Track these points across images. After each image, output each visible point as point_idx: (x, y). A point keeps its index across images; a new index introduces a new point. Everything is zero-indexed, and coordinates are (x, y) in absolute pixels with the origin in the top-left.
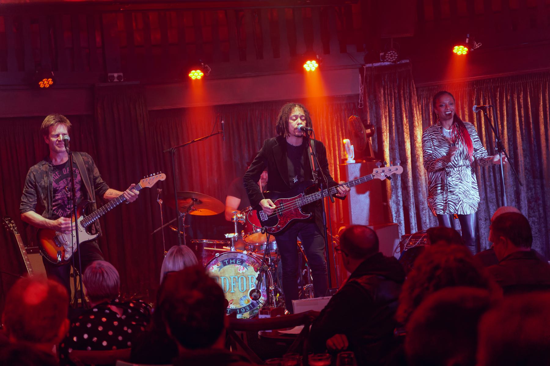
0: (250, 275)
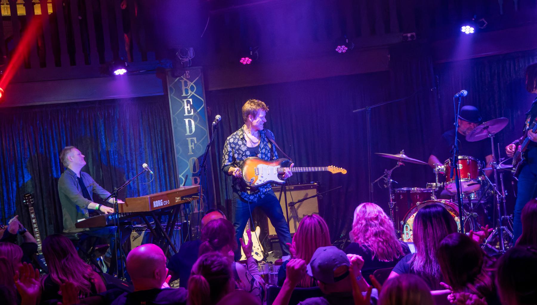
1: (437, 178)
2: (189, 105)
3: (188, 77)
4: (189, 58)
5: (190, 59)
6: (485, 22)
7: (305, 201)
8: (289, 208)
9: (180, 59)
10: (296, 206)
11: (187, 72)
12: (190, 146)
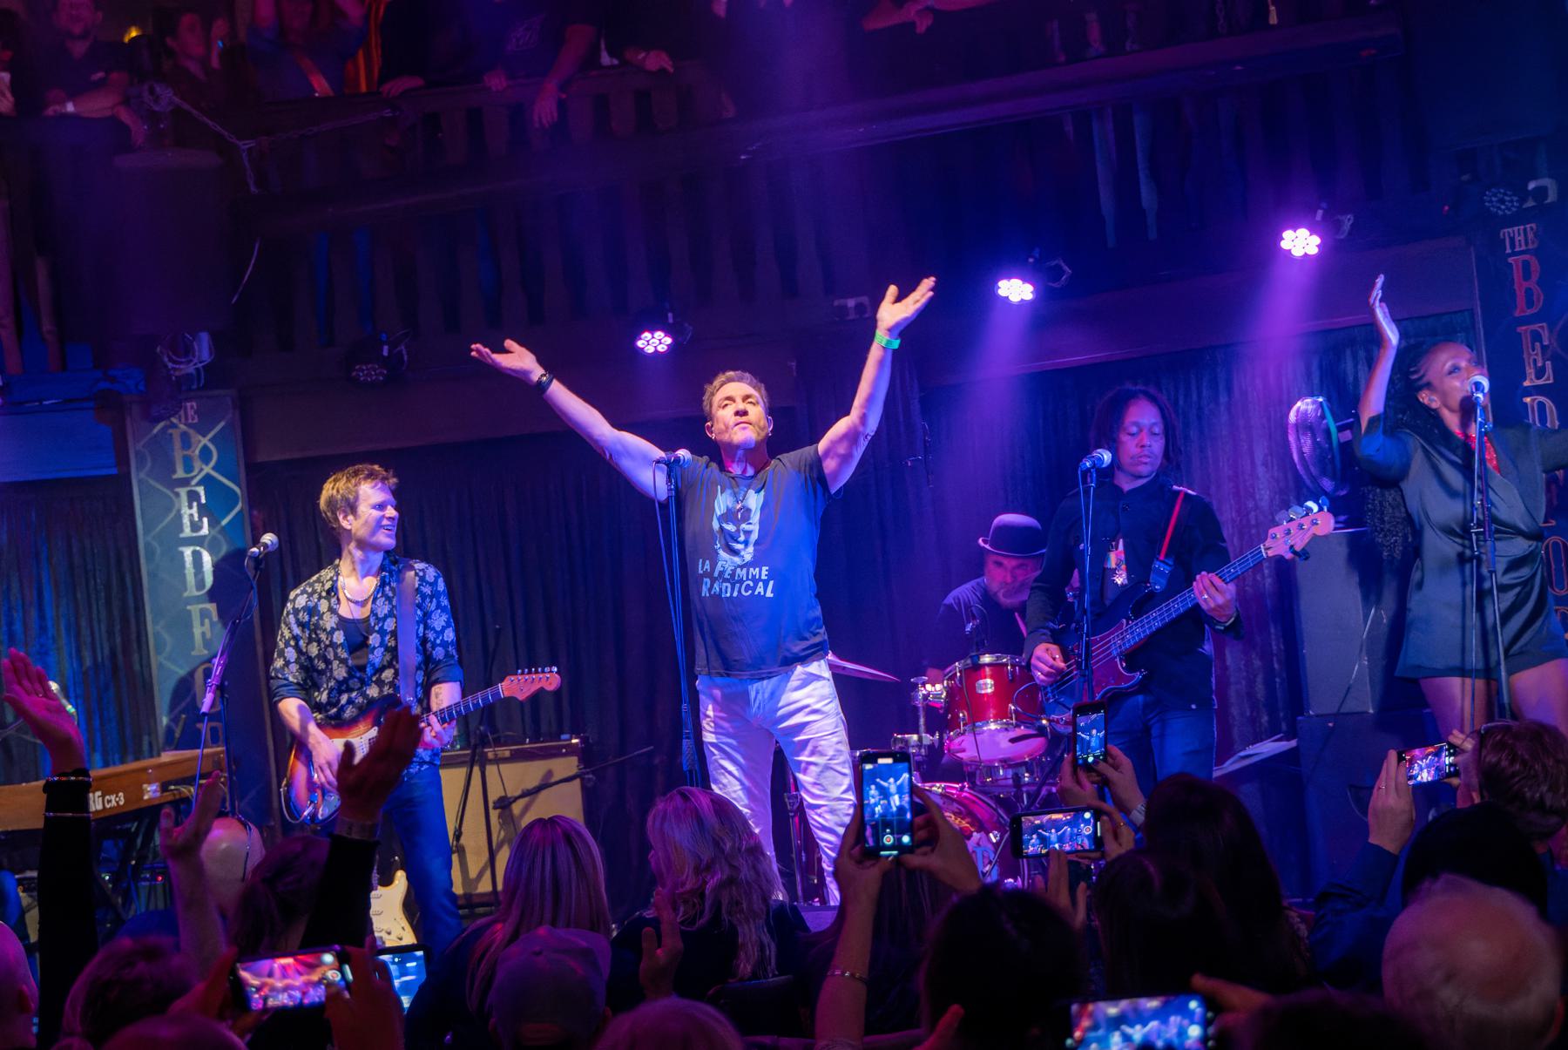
1: (922, 721)
2: (195, 504)
4: (195, 365)
5: (200, 365)
7: (544, 794)
8: (494, 815)
9: (170, 365)
10: (517, 808)
12: (197, 631)
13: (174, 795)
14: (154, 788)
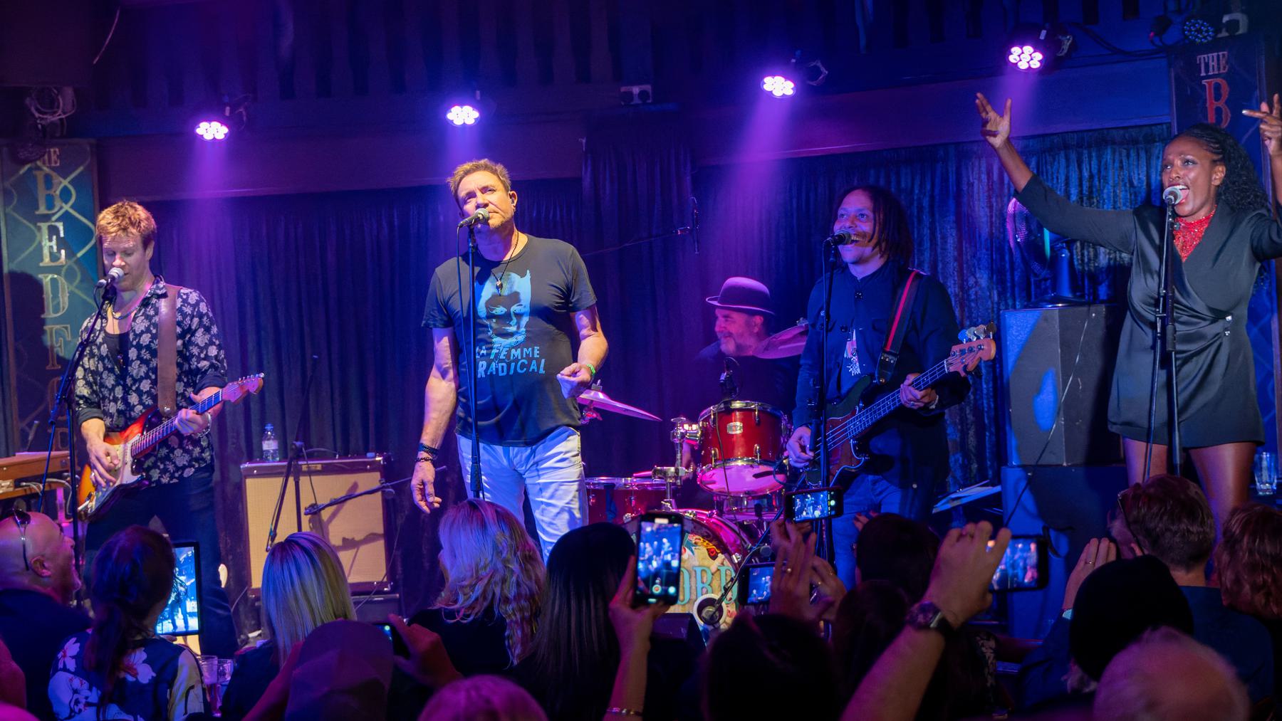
0: (699, 566)
2: (54, 237)
3: (56, 163)
5: (63, 117)
6: (823, 69)
7: (349, 504)
8: (305, 519)
9: (37, 115)
10: (325, 514)
11: (52, 150)
13: (25, 490)
14: (8, 483)
